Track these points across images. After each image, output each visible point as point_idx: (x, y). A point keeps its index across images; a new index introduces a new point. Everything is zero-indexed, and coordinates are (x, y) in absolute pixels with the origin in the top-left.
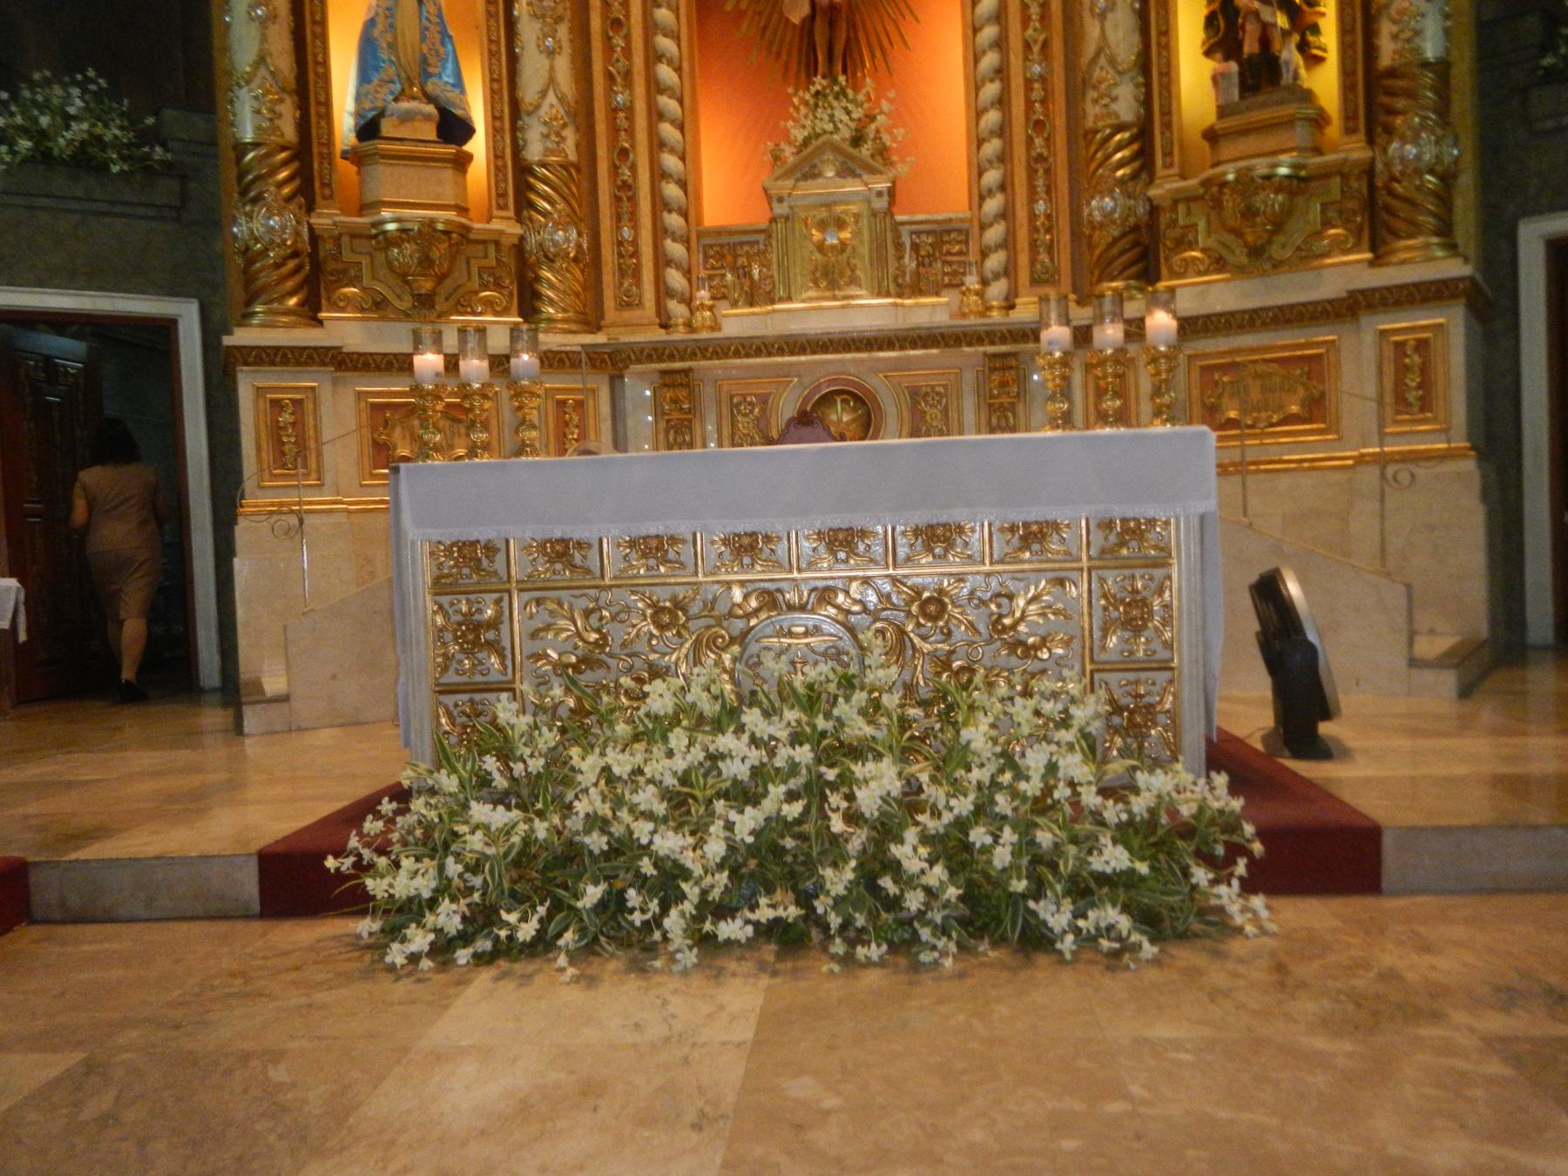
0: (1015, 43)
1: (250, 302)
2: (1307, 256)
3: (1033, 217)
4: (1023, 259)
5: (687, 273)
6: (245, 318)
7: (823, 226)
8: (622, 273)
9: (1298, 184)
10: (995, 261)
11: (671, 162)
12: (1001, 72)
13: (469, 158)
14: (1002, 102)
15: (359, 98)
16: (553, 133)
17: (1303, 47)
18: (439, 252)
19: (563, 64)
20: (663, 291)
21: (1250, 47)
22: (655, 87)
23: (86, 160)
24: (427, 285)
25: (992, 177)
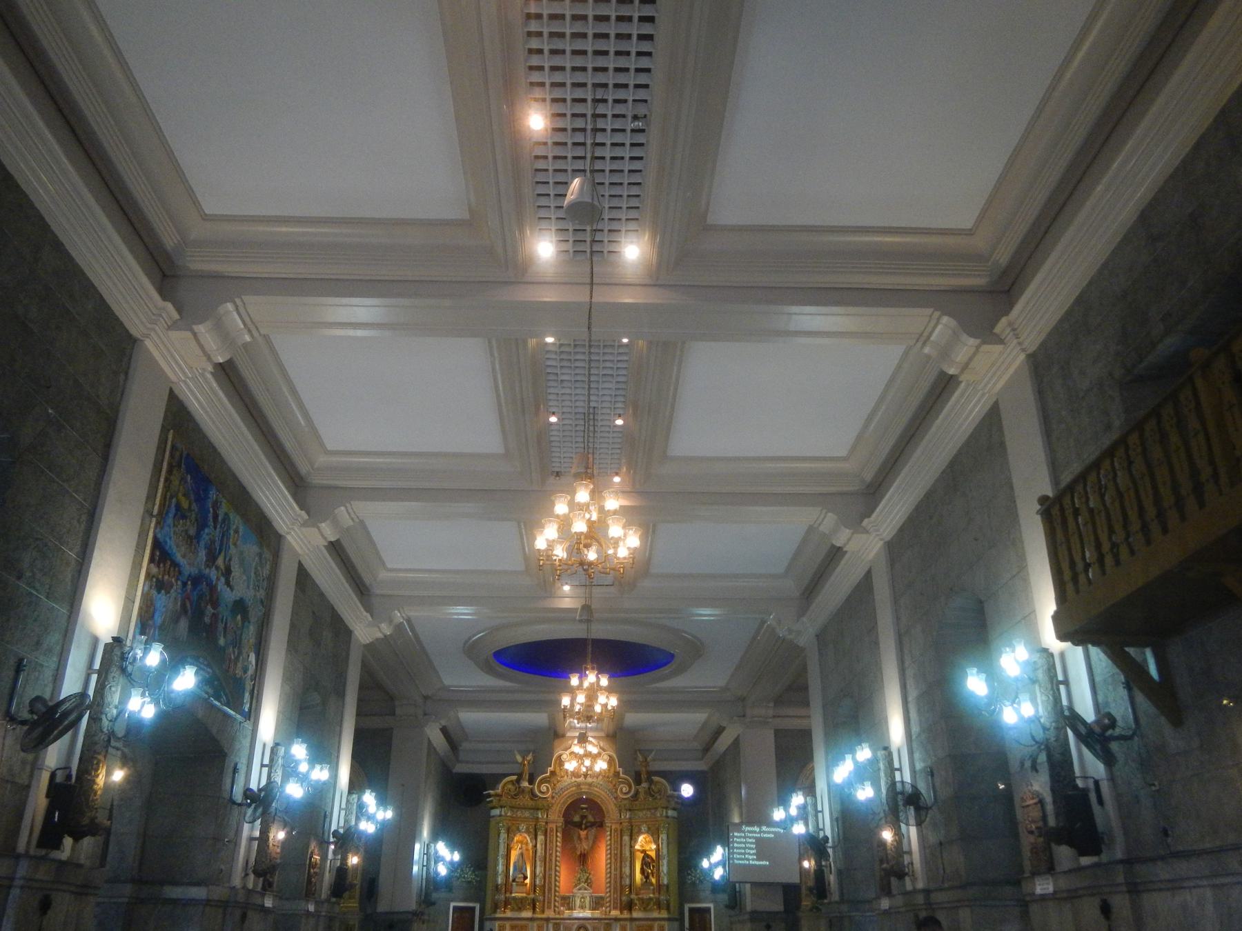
0: (613, 868)
1: (498, 908)
2: (651, 910)
3: (614, 898)
4: (612, 905)
5: (558, 902)
6: (495, 912)
7: (583, 898)
8: (548, 902)
9: (651, 899)
10: (608, 904)
11: (557, 884)
12: (610, 872)
13: (527, 884)
14: (610, 877)
15: (513, 875)
16: (540, 881)
17: (653, 876)
18: (523, 901)
19: (543, 869)
20: (555, 906)
21: (646, 874)
22: (556, 871)
23: (469, 882)
24: (520, 905)
25: (608, 890)
